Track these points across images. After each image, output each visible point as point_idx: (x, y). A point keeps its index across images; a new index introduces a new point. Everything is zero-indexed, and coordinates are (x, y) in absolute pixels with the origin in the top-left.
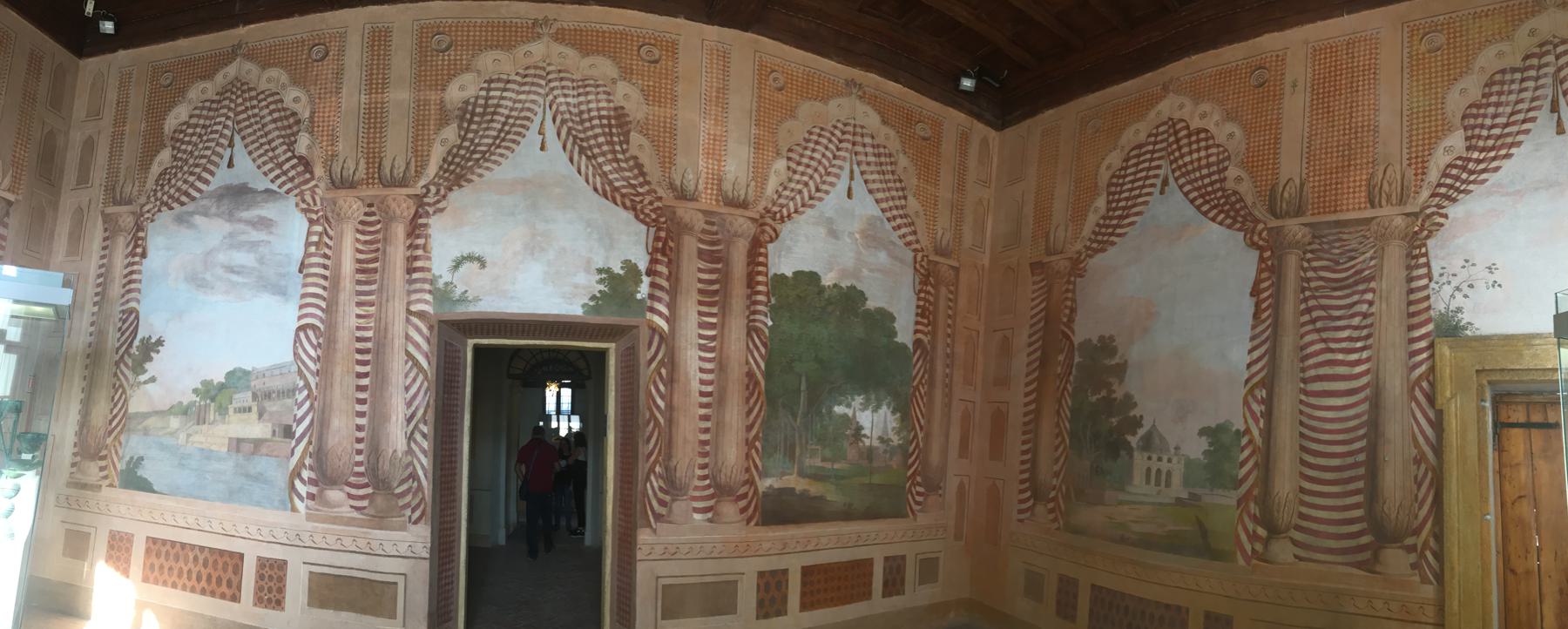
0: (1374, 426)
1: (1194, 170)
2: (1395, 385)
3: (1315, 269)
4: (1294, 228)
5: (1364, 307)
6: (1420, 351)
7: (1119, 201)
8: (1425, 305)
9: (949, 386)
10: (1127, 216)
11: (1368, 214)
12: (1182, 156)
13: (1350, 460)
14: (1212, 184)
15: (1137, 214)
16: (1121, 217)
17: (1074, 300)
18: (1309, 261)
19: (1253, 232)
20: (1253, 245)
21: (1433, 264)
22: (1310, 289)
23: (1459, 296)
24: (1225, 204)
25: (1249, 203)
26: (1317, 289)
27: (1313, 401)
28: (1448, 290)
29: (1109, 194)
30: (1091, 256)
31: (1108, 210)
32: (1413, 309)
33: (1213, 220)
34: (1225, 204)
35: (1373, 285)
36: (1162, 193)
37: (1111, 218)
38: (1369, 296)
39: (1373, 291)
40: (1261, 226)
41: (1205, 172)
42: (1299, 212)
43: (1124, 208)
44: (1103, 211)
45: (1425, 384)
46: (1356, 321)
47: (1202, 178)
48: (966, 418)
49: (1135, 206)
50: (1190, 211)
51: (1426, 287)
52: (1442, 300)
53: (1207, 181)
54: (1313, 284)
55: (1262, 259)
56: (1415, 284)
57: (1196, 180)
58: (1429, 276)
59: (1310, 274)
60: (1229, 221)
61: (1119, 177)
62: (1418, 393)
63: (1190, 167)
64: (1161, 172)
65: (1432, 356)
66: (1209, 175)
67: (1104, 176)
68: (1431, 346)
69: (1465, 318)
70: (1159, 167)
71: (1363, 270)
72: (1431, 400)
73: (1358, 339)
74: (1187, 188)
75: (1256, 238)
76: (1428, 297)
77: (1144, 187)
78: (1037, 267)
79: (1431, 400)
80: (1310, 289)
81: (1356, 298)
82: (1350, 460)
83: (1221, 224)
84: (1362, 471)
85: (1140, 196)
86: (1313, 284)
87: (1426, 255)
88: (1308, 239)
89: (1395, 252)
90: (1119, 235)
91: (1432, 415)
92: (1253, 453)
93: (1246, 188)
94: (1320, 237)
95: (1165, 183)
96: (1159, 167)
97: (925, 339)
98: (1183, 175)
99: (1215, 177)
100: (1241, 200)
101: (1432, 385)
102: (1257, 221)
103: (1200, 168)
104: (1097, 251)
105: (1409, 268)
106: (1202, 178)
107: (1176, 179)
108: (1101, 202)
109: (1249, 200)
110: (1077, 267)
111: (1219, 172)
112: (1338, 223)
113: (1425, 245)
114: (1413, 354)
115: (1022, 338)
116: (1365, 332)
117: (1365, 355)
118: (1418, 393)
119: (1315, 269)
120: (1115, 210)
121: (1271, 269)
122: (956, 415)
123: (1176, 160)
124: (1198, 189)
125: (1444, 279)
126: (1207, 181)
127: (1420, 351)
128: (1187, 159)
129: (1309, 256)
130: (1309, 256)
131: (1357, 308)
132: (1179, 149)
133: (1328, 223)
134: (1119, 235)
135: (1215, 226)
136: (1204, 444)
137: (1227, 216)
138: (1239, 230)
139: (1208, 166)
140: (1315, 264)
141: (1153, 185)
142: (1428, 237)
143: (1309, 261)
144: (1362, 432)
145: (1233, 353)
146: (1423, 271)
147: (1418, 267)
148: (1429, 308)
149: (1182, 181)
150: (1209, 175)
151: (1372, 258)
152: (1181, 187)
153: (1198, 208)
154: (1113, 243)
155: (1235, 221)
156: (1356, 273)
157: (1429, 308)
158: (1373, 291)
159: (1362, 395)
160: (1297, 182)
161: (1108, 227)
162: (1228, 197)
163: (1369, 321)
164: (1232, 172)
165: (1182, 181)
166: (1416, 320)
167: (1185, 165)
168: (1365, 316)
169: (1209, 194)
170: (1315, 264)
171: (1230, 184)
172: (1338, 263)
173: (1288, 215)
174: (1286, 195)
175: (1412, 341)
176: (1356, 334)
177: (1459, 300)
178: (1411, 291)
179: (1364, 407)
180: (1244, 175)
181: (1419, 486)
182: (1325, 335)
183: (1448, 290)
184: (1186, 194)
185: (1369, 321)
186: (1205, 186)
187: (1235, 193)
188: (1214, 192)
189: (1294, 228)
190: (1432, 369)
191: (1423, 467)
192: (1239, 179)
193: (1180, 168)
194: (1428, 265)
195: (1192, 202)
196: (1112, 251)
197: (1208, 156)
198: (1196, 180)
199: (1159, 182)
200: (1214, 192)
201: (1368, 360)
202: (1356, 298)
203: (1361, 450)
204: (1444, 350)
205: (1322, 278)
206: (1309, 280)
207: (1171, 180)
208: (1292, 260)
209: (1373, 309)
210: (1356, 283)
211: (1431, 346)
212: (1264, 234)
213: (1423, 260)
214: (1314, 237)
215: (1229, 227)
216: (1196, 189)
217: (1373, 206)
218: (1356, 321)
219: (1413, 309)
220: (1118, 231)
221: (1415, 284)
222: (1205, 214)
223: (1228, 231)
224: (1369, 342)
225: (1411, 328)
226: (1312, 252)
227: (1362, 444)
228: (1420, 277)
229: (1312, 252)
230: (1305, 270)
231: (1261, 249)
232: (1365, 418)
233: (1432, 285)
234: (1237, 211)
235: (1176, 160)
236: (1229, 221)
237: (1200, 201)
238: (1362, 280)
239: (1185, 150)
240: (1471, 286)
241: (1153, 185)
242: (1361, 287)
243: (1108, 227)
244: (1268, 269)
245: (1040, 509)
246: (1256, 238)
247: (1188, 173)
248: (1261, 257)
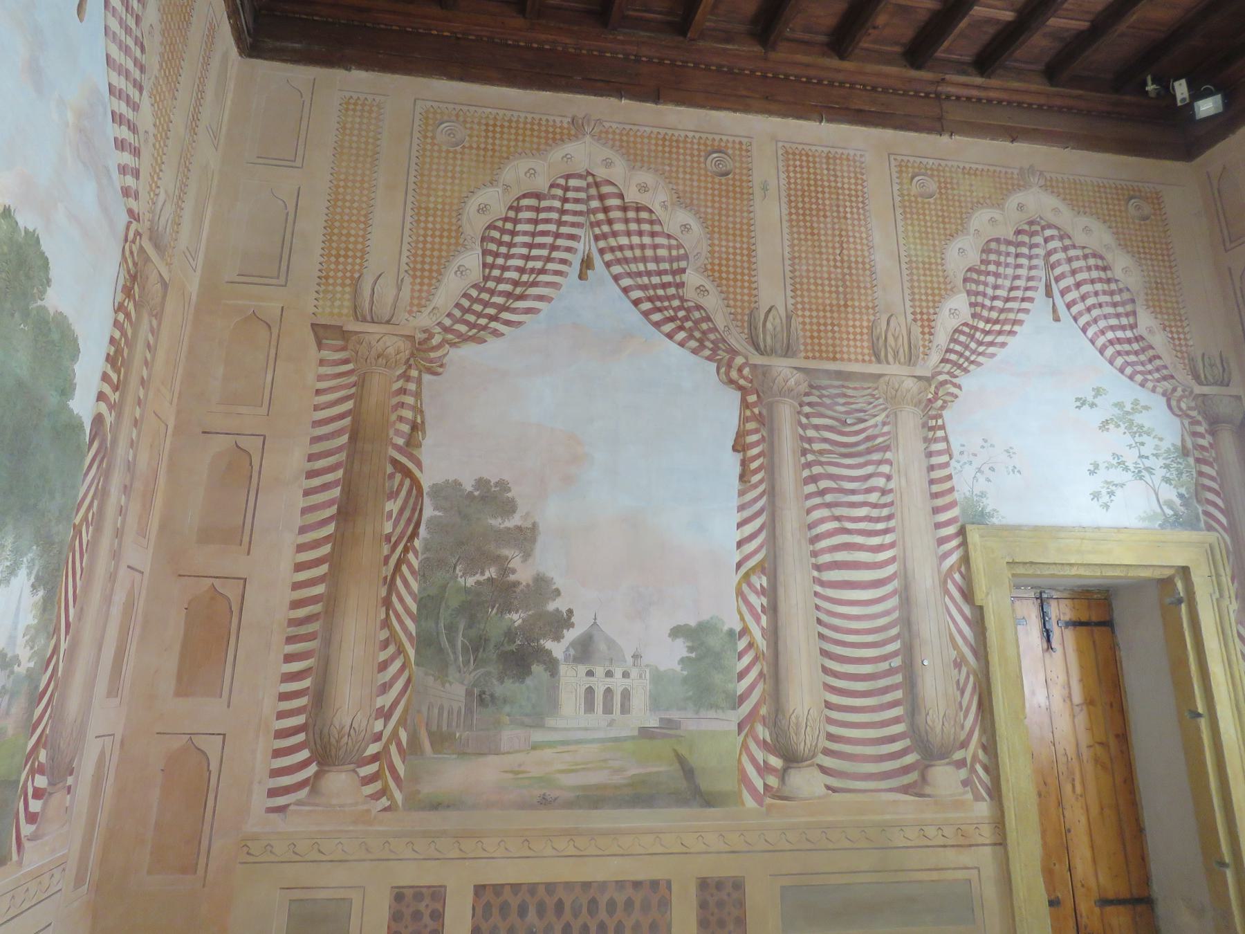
0: (907, 622)
1: (635, 260)
2: (925, 578)
3: (817, 428)
4: (783, 369)
5: (881, 482)
6: (947, 539)
7: (504, 268)
8: (947, 486)
9: (119, 533)
10: (522, 297)
11: (874, 369)
12: (615, 234)
13: (884, 666)
14: (664, 286)
15: (541, 298)
16: (508, 295)
17: (418, 410)
18: (807, 416)
19: (729, 366)
20: (731, 382)
21: (951, 439)
22: (813, 452)
23: (982, 479)
24: (687, 318)
25: (721, 327)
26: (821, 452)
27: (830, 593)
28: (969, 471)
29: (485, 252)
30: (453, 345)
31: (486, 278)
32: (936, 488)
33: (670, 336)
34: (687, 318)
35: (888, 455)
36: (582, 277)
37: (492, 292)
38: (885, 469)
39: (889, 462)
40: (739, 360)
41: (652, 266)
42: (788, 351)
43: (516, 283)
44: (476, 274)
45: (957, 576)
46: (874, 497)
47: (649, 274)
48: (129, 606)
49: (534, 284)
50: (634, 316)
51: (946, 465)
52: (965, 482)
53: (656, 280)
54: (816, 447)
55: (745, 404)
56: (935, 460)
57: (640, 274)
58: (948, 451)
59: (811, 433)
60: (693, 344)
61: (503, 231)
62: (951, 586)
63: (629, 254)
64: (580, 246)
65: (964, 544)
66: (660, 273)
67: (475, 224)
68: (962, 532)
69: (990, 504)
70: (572, 237)
71: (874, 437)
72: (968, 594)
73: (878, 520)
74: (626, 282)
75: (734, 374)
76: (950, 477)
77: (549, 259)
78: (322, 332)
79: (968, 594)
80: (813, 452)
81: (870, 469)
82: (884, 666)
83: (682, 344)
84: (898, 678)
85: (542, 271)
86: (816, 447)
87: (943, 427)
88: (804, 387)
89: (909, 422)
90: (508, 323)
91: (967, 610)
92: (756, 659)
93: (712, 302)
94: (819, 388)
95: (587, 263)
96: (572, 237)
97: (109, 419)
98: (619, 262)
99: (667, 278)
100: (708, 319)
101: (968, 578)
102: (734, 352)
103: (644, 259)
104: (465, 339)
105: (927, 440)
106: (649, 274)
107: (608, 265)
108: (472, 260)
109: (720, 322)
110: (422, 355)
111: (674, 273)
112: (839, 375)
113: (941, 416)
114: (941, 541)
115: (288, 461)
116: (885, 512)
117: (888, 539)
118: (951, 586)
119: (817, 428)
120: (499, 280)
121: (760, 419)
122: (119, 598)
123: (604, 236)
124: (643, 288)
125: (965, 458)
126: (656, 280)
127: (947, 539)
128: (624, 241)
129: (807, 409)
130: (807, 409)
131: (874, 482)
132: (610, 222)
133: (827, 372)
134: (508, 323)
135: (672, 346)
136: (680, 648)
137: (691, 337)
138: (709, 358)
139: (657, 260)
140: (816, 421)
141: (563, 261)
142: (943, 408)
143: (807, 416)
144: (894, 632)
145: (706, 521)
146: (941, 446)
147: (936, 440)
148: (952, 490)
149: (617, 269)
150: (660, 273)
151: (884, 424)
152: (616, 278)
153: (646, 314)
154: (496, 333)
155: (702, 346)
156: (868, 439)
157: (952, 490)
158: (889, 462)
159: (889, 588)
160: (783, 315)
161: (486, 304)
162: (688, 310)
163: (888, 499)
164: (692, 278)
165: (617, 269)
166: (940, 502)
167: (621, 248)
168: (884, 492)
169: (660, 298)
170: (816, 421)
171: (689, 293)
172: (844, 423)
173: (771, 352)
174: (769, 325)
175: (938, 526)
176: (875, 513)
177: (981, 485)
178: (932, 468)
179: (893, 602)
180: (708, 285)
181: (963, 693)
182: (838, 511)
183: (969, 471)
184: (626, 290)
185: (888, 499)
186: (655, 287)
187: (699, 308)
188: (669, 298)
189: (783, 369)
190: (966, 559)
191: (964, 670)
192: (701, 290)
193: (612, 250)
194: (946, 439)
195: (636, 303)
196: (493, 345)
197: (655, 247)
198: (640, 274)
199: (576, 260)
200: (669, 298)
201: (892, 545)
202: (870, 469)
203: (894, 654)
204: (974, 536)
205: (825, 440)
206: (810, 440)
207: (598, 261)
208: (785, 413)
209: (891, 485)
210: (869, 451)
211: (962, 532)
212: (746, 371)
213: (940, 434)
214: (811, 386)
215: (695, 352)
216: (643, 288)
217: (879, 361)
218: (874, 497)
219: (936, 488)
220: (505, 316)
221: (935, 460)
222: (657, 325)
223: (693, 357)
224: (892, 524)
225: (936, 510)
226: (810, 404)
227: (896, 646)
228: (940, 453)
229: (810, 404)
230: (804, 427)
231: (740, 388)
232: (896, 615)
233: (953, 463)
234: (704, 333)
235: (604, 236)
236: (693, 344)
237: (647, 306)
238: (876, 448)
239: (618, 227)
240: (992, 469)
241: (563, 261)
242: (876, 457)
243: (486, 304)
244: (755, 418)
245: (338, 781)
246: (734, 374)
247: (626, 261)
248: (743, 400)
